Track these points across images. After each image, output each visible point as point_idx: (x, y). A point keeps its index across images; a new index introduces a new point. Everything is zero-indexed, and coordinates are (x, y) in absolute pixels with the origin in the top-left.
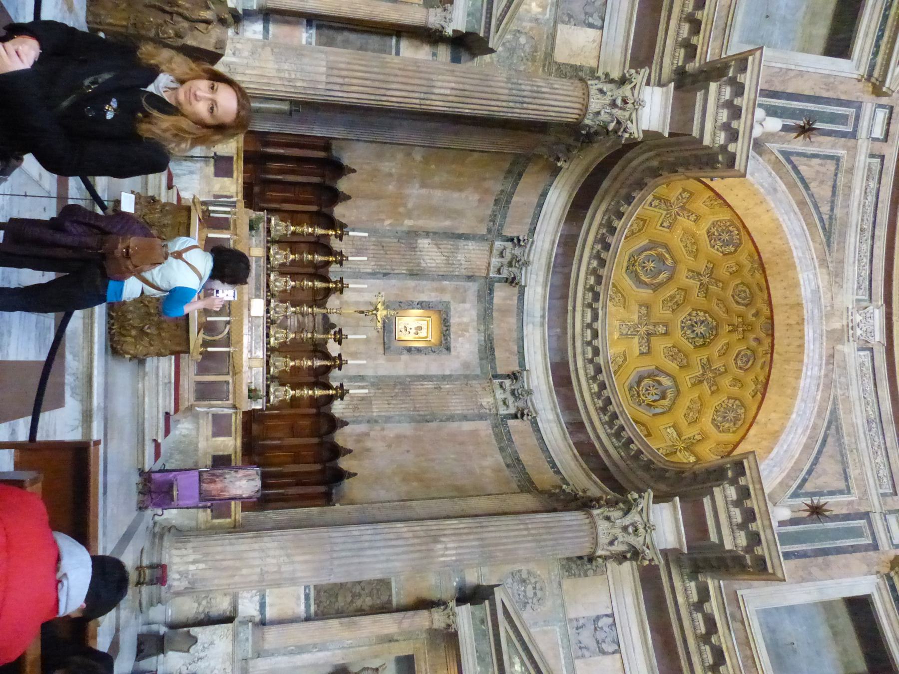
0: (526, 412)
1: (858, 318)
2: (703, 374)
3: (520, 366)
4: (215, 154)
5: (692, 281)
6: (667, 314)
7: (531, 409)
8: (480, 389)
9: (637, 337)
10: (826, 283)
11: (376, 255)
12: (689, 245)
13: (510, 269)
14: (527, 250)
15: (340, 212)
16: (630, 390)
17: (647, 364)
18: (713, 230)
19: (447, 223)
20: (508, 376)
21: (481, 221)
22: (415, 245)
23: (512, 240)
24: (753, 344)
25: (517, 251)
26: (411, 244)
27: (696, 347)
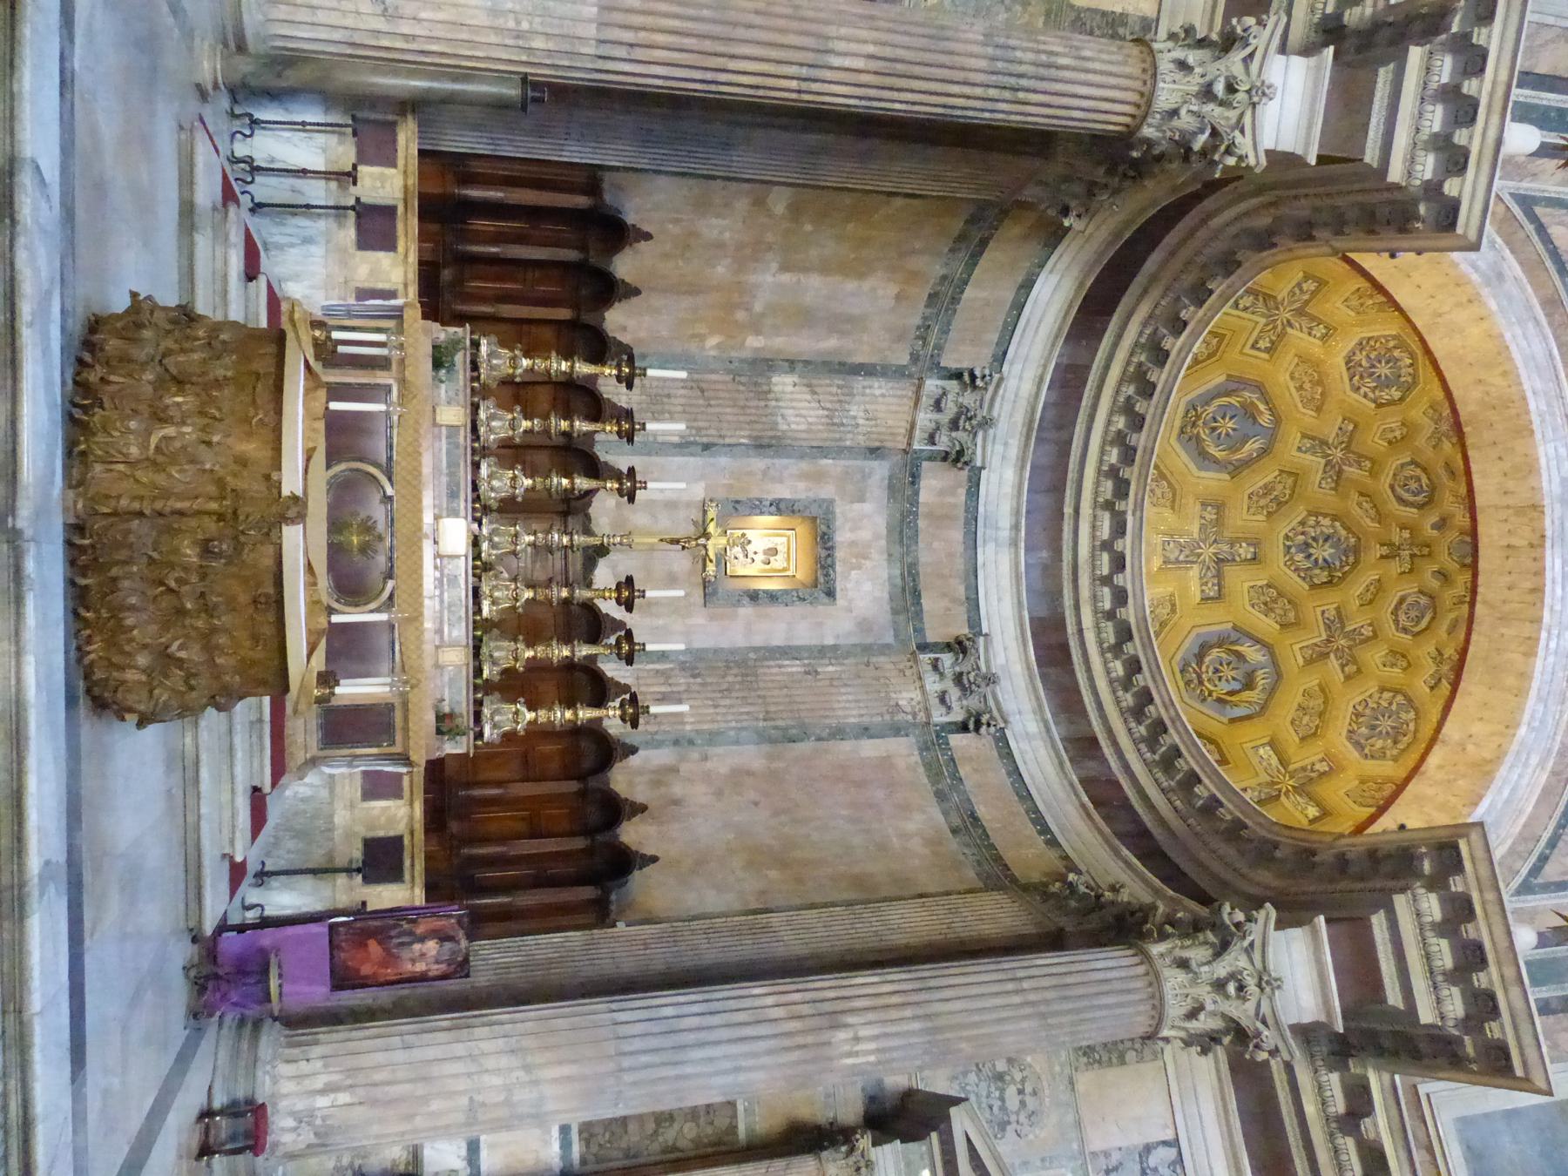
0: (984, 719)
2: (1328, 641)
3: (970, 627)
4: (358, 199)
7: (995, 713)
8: (895, 673)
11: (687, 409)
12: (1307, 386)
13: (954, 434)
15: (618, 321)
18: (1360, 357)
20: (948, 647)
22: (765, 388)
24: (1435, 584)
25: (969, 399)
26: (756, 384)
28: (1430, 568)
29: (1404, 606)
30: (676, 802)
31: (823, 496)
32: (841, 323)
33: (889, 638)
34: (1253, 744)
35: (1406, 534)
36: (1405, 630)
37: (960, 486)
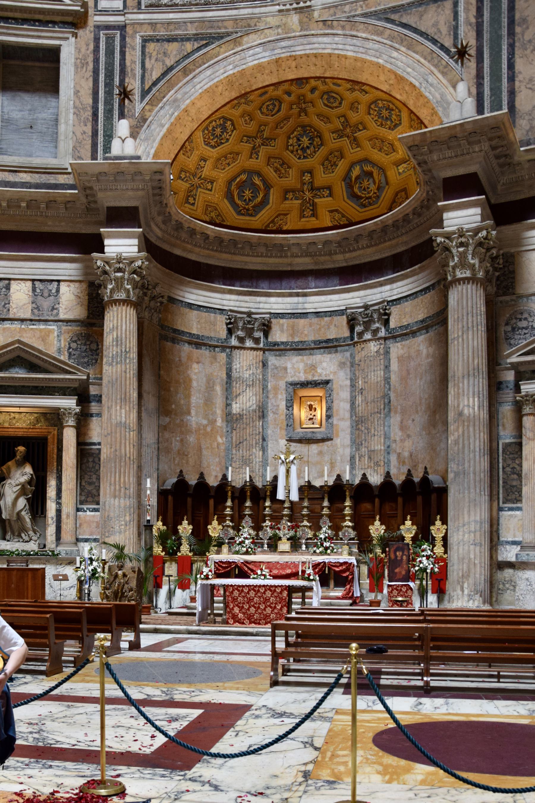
3: (343, 315)
5: (260, 154)
6: (293, 173)
8: (363, 352)
9: (316, 200)
10: (257, 36)
14: (239, 315)
15: (213, 481)
16: (364, 206)
17: (340, 189)
19: (218, 389)
21: (215, 359)
22: (238, 416)
23: (230, 332)
24: (317, 93)
26: (237, 420)
27: (322, 144)
28: (309, 96)
29: (329, 104)
31: (284, 387)
32: (210, 386)
33: (348, 354)
34: (397, 174)
35: (294, 106)
36: (340, 103)
37: (279, 323)
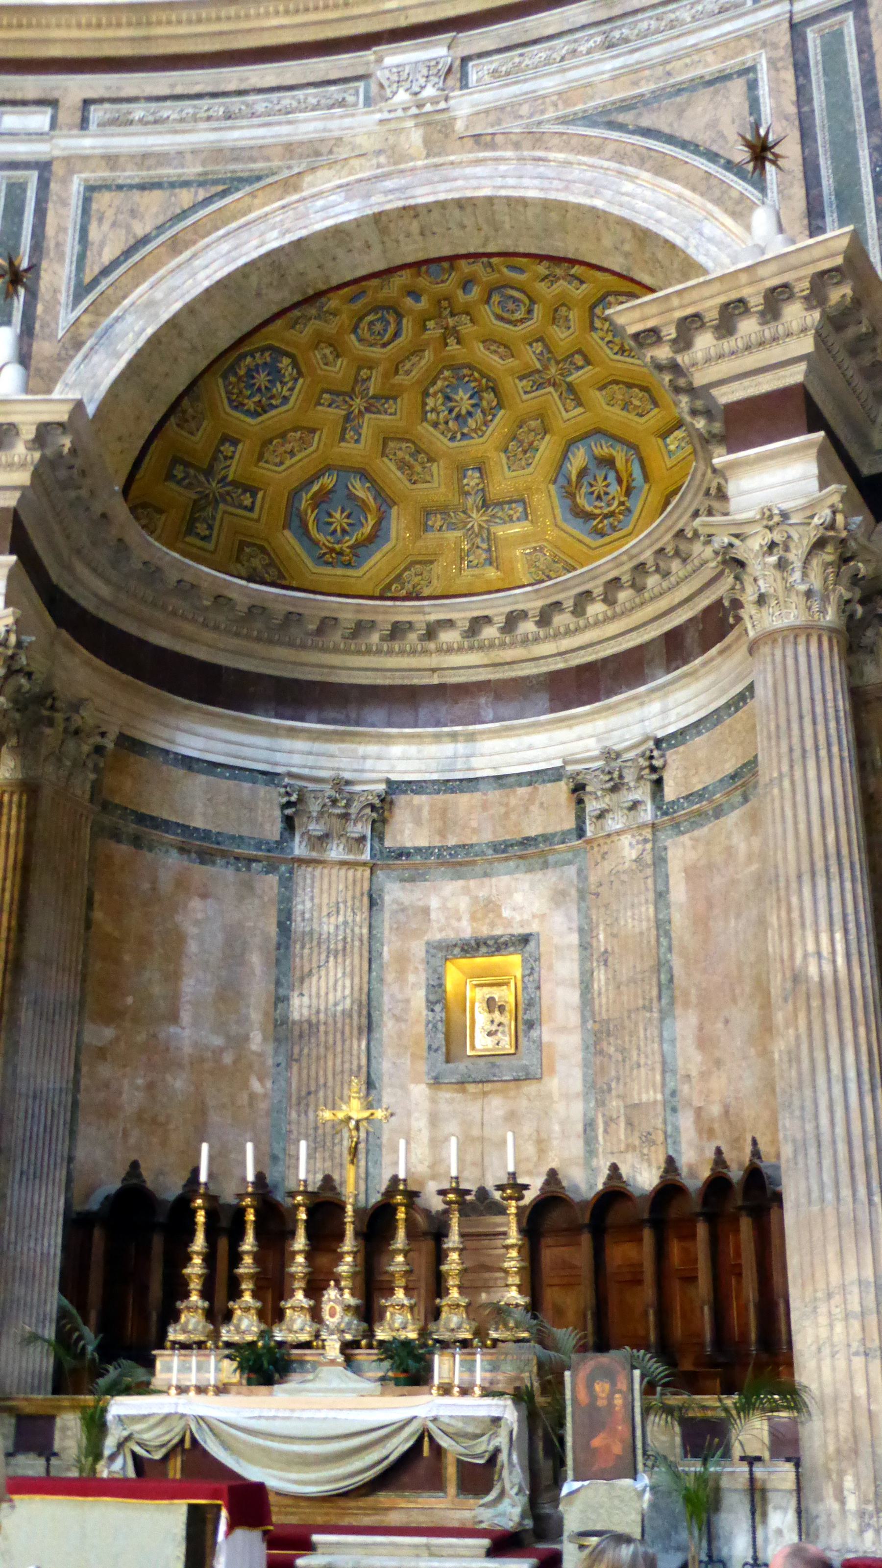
1: (402, 96)
24: (476, 292)
28: (461, 297)
30: (726, 1112)
33: (571, 871)
36: (530, 311)
